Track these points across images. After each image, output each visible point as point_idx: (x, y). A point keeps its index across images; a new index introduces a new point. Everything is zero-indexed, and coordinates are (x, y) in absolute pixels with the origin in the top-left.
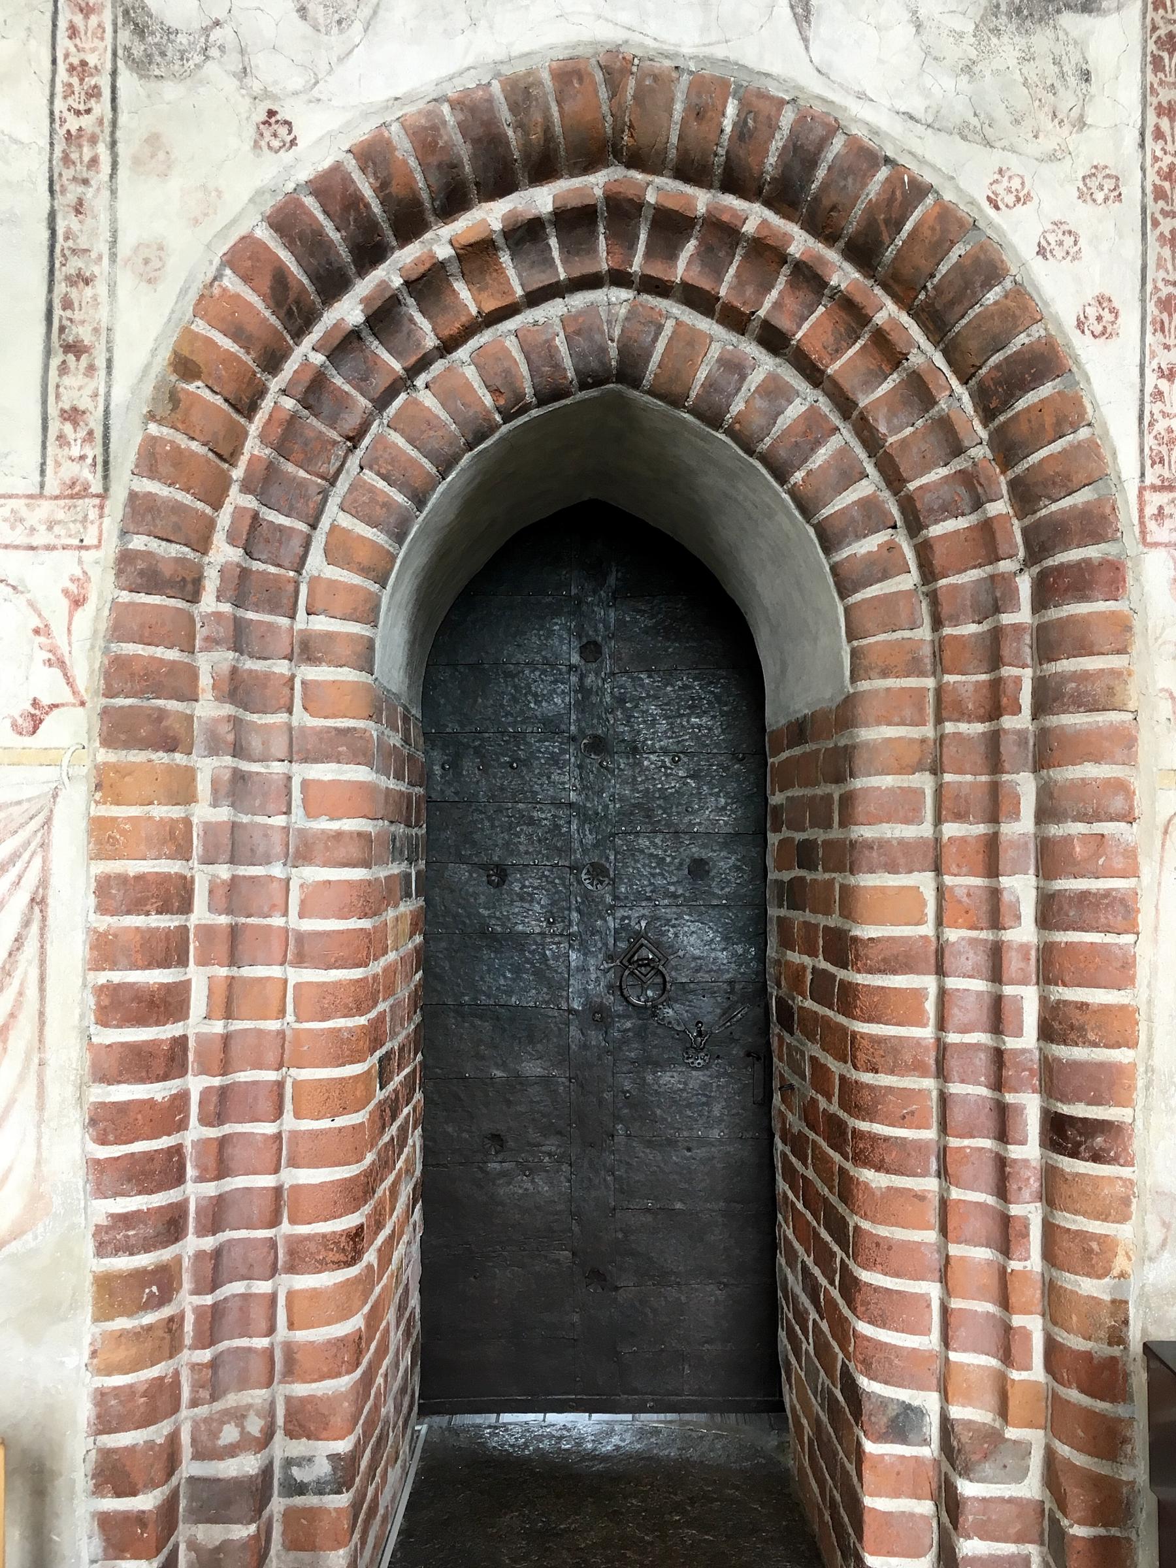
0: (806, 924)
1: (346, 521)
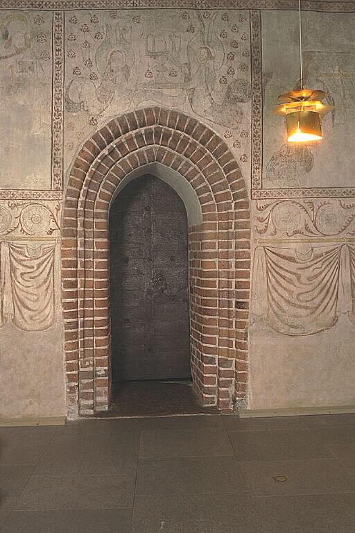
0: (195, 270)
1: (103, 190)
